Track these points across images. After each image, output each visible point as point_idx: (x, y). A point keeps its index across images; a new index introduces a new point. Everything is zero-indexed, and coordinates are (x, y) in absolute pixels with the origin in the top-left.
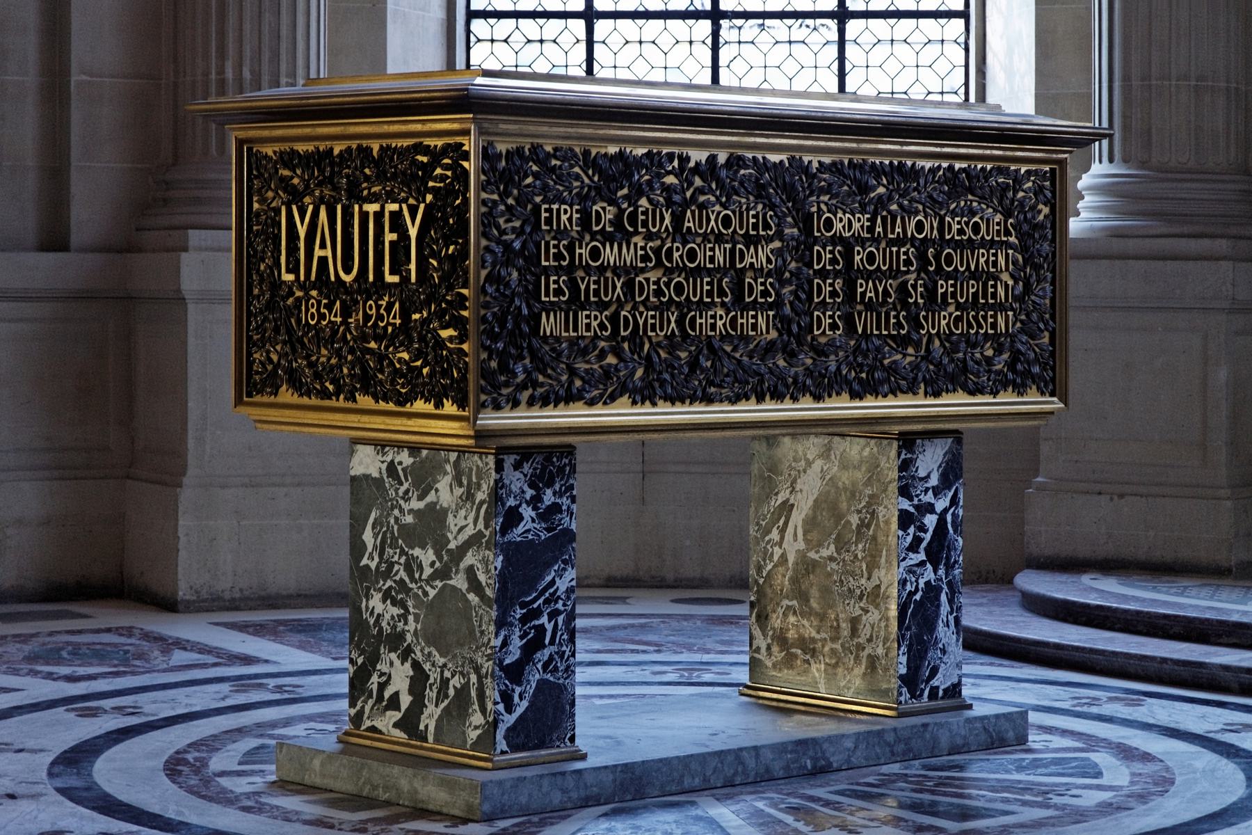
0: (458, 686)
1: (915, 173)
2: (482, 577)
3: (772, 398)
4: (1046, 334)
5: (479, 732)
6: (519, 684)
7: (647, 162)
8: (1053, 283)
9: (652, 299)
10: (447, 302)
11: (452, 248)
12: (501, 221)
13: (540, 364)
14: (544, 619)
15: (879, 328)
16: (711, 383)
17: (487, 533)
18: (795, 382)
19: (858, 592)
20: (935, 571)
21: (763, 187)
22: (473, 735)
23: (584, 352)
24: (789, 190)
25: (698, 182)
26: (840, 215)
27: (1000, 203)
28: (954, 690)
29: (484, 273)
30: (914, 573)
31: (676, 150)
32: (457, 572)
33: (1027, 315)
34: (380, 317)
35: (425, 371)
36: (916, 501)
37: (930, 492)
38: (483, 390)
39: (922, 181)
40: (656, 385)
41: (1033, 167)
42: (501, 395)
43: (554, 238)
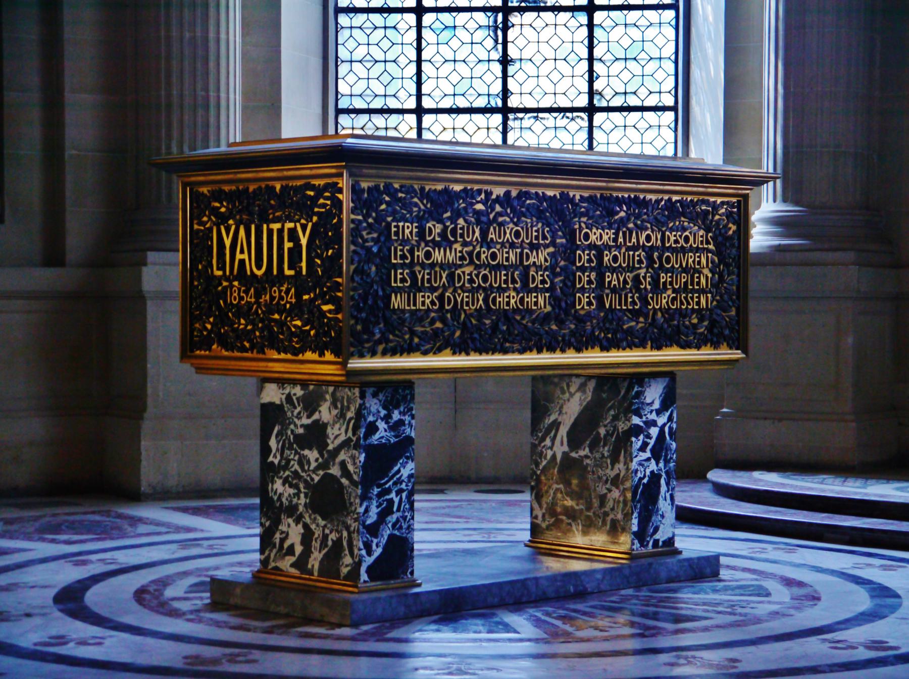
0: (335, 539)
1: (645, 203)
2: (351, 468)
3: (547, 351)
4: (734, 309)
5: (349, 568)
6: (376, 537)
7: (463, 195)
8: (738, 276)
9: (467, 285)
10: (327, 287)
11: (330, 251)
12: (364, 233)
13: (391, 327)
14: (393, 495)
15: (620, 304)
16: (506, 340)
17: (354, 439)
18: (563, 340)
19: (605, 478)
20: (657, 464)
21: (542, 212)
22: (345, 570)
23: (421, 320)
24: (560, 214)
25: (498, 208)
26: (594, 230)
27: (703, 223)
28: (670, 542)
29: (352, 267)
30: (643, 465)
31: (485, 187)
32: (334, 464)
33: (721, 297)
34: (281, 298)
35: (312, 333)
36: (644, 419)
37: (654, 413)
38: (352, 345)
39: (650, 209)
40: (469, 341)
41: (726, 199)
42: (364, 347)
43: (400, 245)
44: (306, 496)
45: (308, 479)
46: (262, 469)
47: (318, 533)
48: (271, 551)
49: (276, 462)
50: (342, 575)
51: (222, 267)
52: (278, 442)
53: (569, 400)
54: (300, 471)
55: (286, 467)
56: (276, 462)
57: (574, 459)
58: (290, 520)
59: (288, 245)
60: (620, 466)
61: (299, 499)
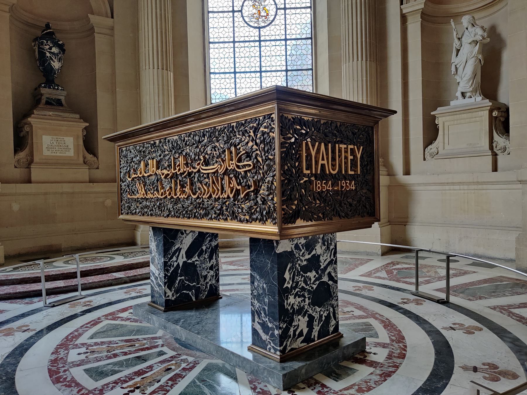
0: (326, 315)
17: (334, 259)
22: (331, 329)
47: (316, 316)
48: (288, 341)
49: (289, 286)
50: (331, 332)
51: (309, 167)
54: (305, 286)
55: (295, 288)
56: (289, 286)
57: (190, 263)
58: (300, 317)
59: (350, 157)
60: (214, 261)
61: (305, 302)
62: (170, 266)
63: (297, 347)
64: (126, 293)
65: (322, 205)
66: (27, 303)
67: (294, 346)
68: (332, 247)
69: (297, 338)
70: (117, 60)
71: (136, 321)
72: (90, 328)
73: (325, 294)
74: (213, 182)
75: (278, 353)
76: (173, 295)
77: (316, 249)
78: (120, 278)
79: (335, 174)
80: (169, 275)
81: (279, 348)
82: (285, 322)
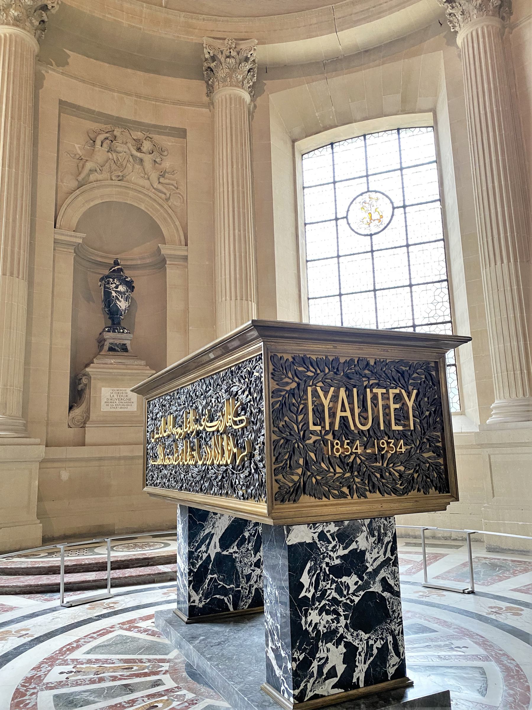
0: (380, 646)
17: (393, 558)
19: (250, 563)
22: (391, 671)
44: (346, 617)
45: (348, 602)
46: (292, 606)
47: (361, 647)
49: (310, 595)
50: (390, 675)
52: (311, 578)
53: (220, 518)
54: (338, 597)
56: (310, 595)
58: (329, 645)
61: (338, 622)
62: (197, 558)
63: (327, 695)
64: (164, 594)
65: (348, 475)
66: (46, 600)
67: (319, 691)
68: (386, 539)
69: (326, 679)
70: (190, 294)
71: (153, 634)
72: (95, 639)
73: (377, 612)
74: (215, 444)
75: (292, 699)
76: (200, 601)
77: (357, 542)
78: (165, 573)
79: (368, 430)
80: (195, 570)
81: (292, 691)
82: (304, 650)
